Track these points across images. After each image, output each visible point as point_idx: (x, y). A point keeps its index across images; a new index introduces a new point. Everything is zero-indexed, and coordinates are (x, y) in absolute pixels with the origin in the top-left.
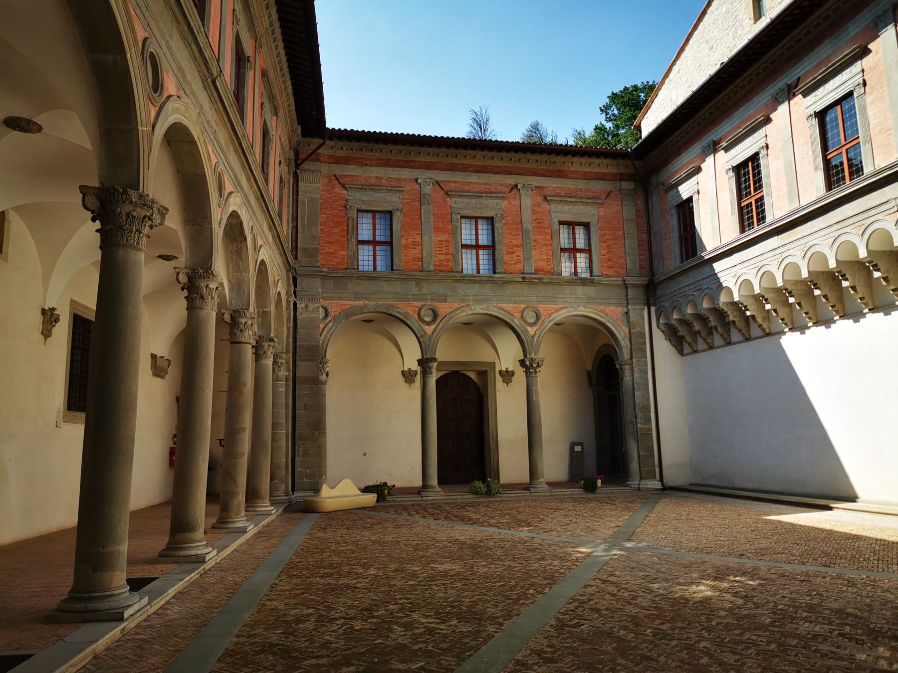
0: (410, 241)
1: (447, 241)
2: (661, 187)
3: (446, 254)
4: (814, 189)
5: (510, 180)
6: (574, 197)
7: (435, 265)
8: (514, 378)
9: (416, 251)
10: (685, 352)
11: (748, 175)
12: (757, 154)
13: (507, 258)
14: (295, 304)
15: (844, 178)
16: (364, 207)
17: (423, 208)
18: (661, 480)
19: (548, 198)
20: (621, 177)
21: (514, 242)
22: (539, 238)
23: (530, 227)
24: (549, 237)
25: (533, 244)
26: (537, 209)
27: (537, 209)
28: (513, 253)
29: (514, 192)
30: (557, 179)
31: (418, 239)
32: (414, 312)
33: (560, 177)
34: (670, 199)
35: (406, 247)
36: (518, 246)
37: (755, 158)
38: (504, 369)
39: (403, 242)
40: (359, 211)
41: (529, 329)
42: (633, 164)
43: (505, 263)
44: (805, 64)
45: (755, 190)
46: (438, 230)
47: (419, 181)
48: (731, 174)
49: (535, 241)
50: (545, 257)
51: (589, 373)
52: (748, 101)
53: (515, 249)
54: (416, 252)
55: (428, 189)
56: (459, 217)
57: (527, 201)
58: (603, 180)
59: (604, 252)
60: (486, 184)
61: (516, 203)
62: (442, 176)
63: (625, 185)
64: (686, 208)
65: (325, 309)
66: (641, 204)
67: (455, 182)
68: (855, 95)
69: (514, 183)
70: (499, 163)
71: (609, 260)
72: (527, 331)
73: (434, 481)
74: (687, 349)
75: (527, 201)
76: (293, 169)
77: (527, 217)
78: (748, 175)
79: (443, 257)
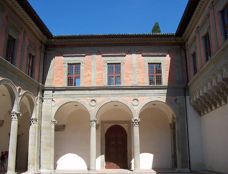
0: (87, 74)
1: (102, 73)
7: (96, 83)
10: (202, 114)
13: (126, 79)
18: (190, 168)
21: (129, 72)
24: (143, 70)
25: (137, 72)
26: (139, 59)
27: (139, 59)
31: (90, 73)
35: (85, 76)
36: (131, 74)
39: (84, 75)
42: (175, 38)
43: (125, 81)
46: (98, 69)
50: (142, 78)
53: (129, 75)
54: (88, 78)
76: (43, 50)
79: (100, 80)
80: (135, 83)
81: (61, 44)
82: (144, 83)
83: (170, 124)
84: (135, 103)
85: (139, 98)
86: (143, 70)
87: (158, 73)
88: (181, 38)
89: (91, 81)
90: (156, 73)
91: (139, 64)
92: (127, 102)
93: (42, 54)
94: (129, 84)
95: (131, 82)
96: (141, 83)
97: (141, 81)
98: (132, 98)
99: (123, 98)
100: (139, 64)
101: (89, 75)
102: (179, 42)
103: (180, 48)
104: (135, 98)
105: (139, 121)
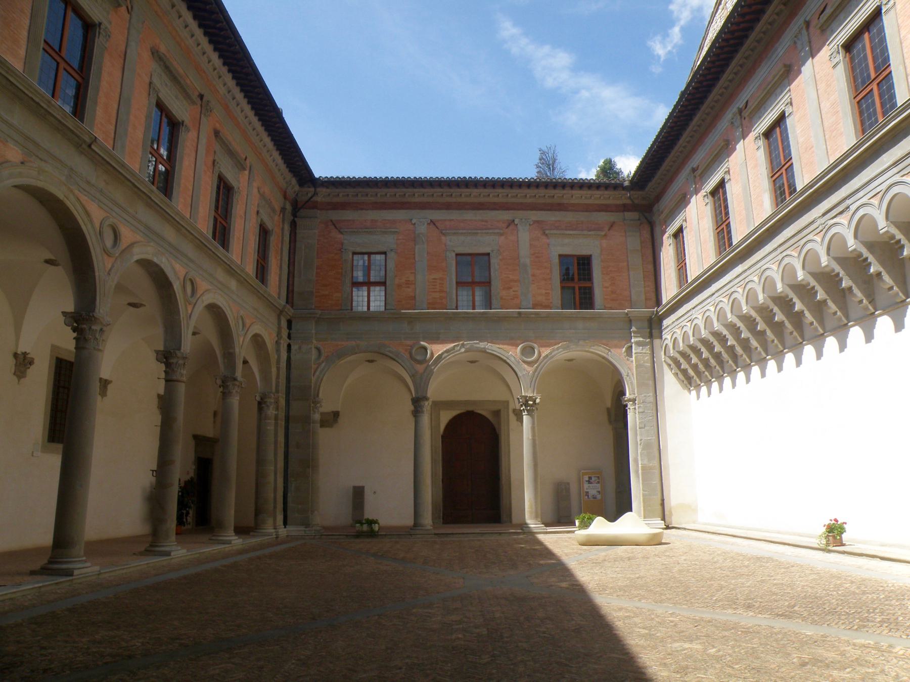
3: (441, 291)
5: (506, 215)
6: (575, 229)
14: (289, 346)
16: (358, 250)
17: (417, 247)
19: (547, 232)
20: (625, 208)
23: (528, 261)
28: (510, 288)
29: (510, 228)
30: (557, 213)
31: (412, 278)
33: (560, 210)
40: (354, 253)
43: (501, 298)
47: (413, 221)
49: (533, 275)
50: (544, 291)
55: (422, 229)
56: (454, 254)
57: (524, 235)
58: (607, 211)
59: (607, 285)
60: (482, 221)
62: (436, 215)
63: (628, 215)
65: (319, 350)
66: (646, 235)
67: (450, 220)
69: (511, 219)
71: (613, 292)
73: (427, 519)
75: (524, 235)
76: (289, 217)
77: (524, 251)
81: (335, 200)
83: (608, 410)
87: (584, 279)
88: (640, 193)
89: (414, 298)
90: (580, 280)
91: (537, 257)
92: (506, 355)
93: (287, 227)
100: (537, 257)
101: (408, 283)
102: (636, 202)
103: (637, 217)
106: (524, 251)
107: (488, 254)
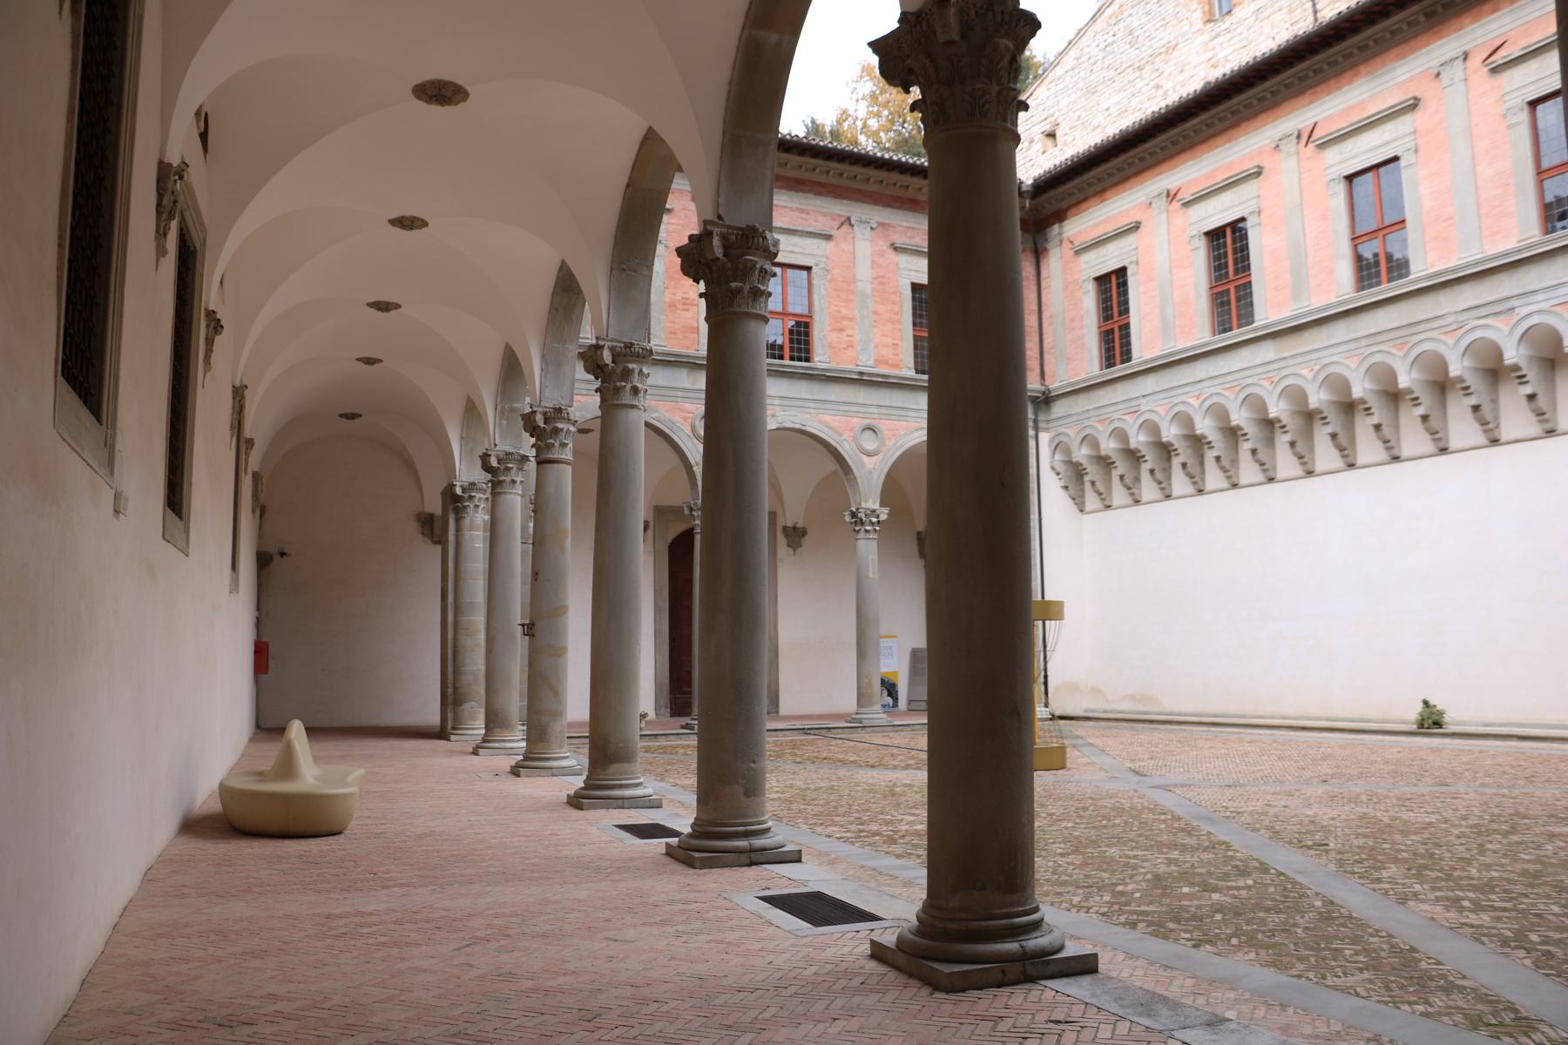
0: (679, 296)
2: (1066, 245)
4: (1340, 284)
8: (806, 541)
9: (688, 315)
10: (1088, 507)
11: (1228, 246)
12: (1243, 219)
13: (833, 337)
15: (1378, 274)
21: (844, 312)
22: (881, 308)
26: (880, 260)
27: (880, 260)
28: (841, 330)
29: (846, 227)
32: (685, 419)
34: (1084, 266)
35: (672, 306)
36: (851, 319)
37: (1237, 229)
38: (790, 524)
39: (668, 297)
41: (865, 458)
44: (1327, 106)
45: (1236, 272)
48: (1202, 245)
49: (875, 313)
50: (890, 341)
51: (920, 538)
52: (1230, 140)
53: (845, 323)
61: (846, 246)
64: (1113, 286)
68: (1402, 163)
70: (823, 179)
72: (863, 464)
74: (1091, 500)
77: (864, 273)
78: (1228, 246)
80: (866, 362)
82: (896, 366)
84: (869, 443)
85: (883, 425)
86: (896, 309)
91: (882, 283)
94: (845, 364)
95: (850, 353)
96: (886, 363)
97: (887, 352)
98: (858, 422)
99: (826, 418)
104: (867, 422)
105: (883, 517)
106: (864, 273)
107: (809, 269)
